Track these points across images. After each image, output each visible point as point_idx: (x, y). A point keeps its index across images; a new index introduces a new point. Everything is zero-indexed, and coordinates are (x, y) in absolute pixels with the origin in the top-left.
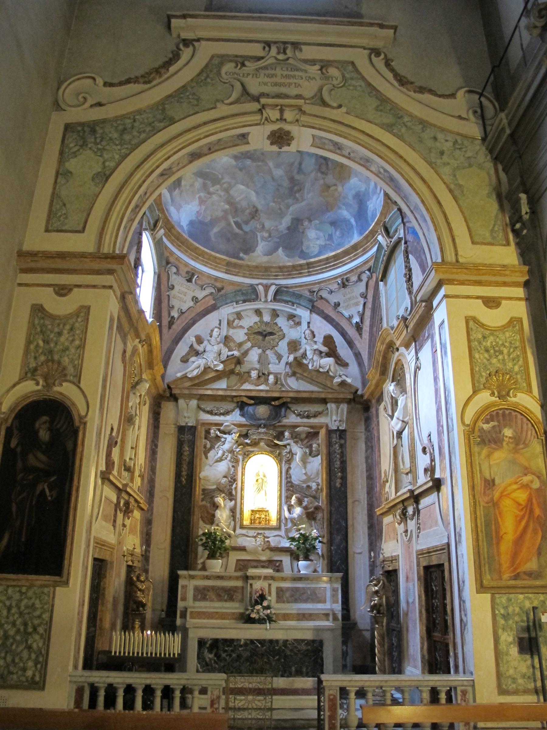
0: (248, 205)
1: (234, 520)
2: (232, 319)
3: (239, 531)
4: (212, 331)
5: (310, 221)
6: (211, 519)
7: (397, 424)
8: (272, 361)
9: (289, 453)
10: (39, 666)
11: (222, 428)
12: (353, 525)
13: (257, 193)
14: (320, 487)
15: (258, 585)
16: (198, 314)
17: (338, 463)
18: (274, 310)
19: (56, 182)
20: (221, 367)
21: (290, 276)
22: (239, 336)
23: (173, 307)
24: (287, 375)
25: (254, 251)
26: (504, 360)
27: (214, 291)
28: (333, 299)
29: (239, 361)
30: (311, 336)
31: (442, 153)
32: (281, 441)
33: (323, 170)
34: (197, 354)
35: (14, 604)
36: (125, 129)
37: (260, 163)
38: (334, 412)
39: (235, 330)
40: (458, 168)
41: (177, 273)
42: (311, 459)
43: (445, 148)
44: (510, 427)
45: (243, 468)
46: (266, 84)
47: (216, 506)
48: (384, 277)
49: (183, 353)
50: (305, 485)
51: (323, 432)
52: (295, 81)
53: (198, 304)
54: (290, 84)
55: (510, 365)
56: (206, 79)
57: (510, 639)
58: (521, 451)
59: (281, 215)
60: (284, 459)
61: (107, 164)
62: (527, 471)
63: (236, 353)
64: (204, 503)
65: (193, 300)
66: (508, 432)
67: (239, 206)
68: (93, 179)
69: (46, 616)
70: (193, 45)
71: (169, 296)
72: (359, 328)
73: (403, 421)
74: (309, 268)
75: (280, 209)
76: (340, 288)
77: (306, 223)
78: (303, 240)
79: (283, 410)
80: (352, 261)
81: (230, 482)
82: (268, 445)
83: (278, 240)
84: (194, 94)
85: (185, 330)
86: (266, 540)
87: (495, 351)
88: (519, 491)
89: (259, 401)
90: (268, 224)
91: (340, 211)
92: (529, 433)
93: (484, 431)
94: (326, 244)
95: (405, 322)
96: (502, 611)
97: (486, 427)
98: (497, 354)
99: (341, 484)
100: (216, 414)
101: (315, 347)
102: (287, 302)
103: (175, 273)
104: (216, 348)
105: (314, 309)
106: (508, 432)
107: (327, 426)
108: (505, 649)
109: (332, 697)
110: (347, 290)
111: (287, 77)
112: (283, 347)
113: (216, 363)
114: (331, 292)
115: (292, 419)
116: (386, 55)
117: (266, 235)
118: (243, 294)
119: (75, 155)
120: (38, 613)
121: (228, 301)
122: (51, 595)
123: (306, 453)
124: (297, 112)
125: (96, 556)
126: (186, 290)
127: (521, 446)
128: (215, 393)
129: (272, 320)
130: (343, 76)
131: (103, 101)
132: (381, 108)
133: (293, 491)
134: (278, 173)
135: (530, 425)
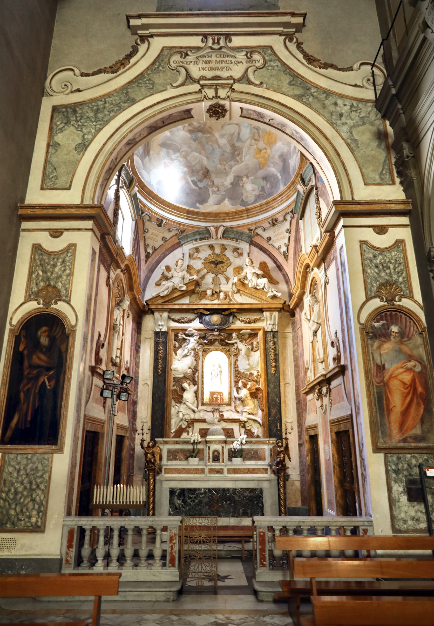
0: (201, 167)
1: (197, 400)
2: (192, 253)
3: (200, 407)
4: (177, 262)
5: (248, 177)
6: (180, 400)
7: (313, 325)
8: (222, 282)
9: (236, 349)
10: (41, 514)
11: (187, 332)
12: (285, 402)
13: (208, 158)
14: (259, 374)
15: (214, 447)
16: (167, 250)
17: (273, 356)
18: (223, 245)
19: (47, 152)
20: (184, 288)
21: (234, 219)
22: (198, 264)
23: (148, 245)
24: (234, 292)
25: (206, 202)
26: (390, 273)
27: (178, 232)
28: (266, 235)
29: (197, 284)
30: (250, 262)
31: (341, 115)
32: (230, 340)
34: (167, 279)
35: (22, 468)
36: (98, 109)
37: (209, 135)
38: (269, 318)
39: (195, 261)
40: (354, 126)
41: (150, 220)
42: (252, 353)
43: (343, 111)
44: (396, 324)
45: (203, 362)
46: (204, 69)
47: (184, 390)
48: (302, 216)
49: (157, 279)
50: (248, 373)
51: (261, 333)
52: (226, 65)
53: (167, 242)
54: (222, 69)
55: (395, 277)
56: (158, 68)
57: (401, 489)
58: (406, 343)
59: (226, 174)
60: (233, 354)
61: (86, 136)
62: (410, 358)
63: (195, 277)
64: (175, 387)
65: (163, 240)
66: (394, 329)
67: (195, 169)
68: (76, 149)
69: (46, 476)
70: (148, 41)
71: (144, 237)
72: (285, 255)
73: (317, 323)
74: (247, 213)
75: (225, 169)
76: (271, 227)
77: (245, 179)
79: (231, 318)
80: (279, 206)
81: (193, 371)
82: (221, 345)
84: (150, 80)
85: (158, 262)
86: (221, 413)
87: (383, 267)
88: (404, 374)
89: (213, 311)
91: (269, 168)
92: (412, 328)
93: (376, 328)
94: (260, 194)
95: (316, 249)
96: (394, 467)
97: (376, 325)
98: (385, 269)
99: (275, 371)
100: (182, 322)
101: (254, 271)
102: (232, 239)
103: (148, 220)
104: (181, 274)
105: (252, 243)
106: (394, 329)
107: (264, 329)
108: (397, 497)
109: (262, 534)
110: (276, 227)
111: (221, 62)
112: (230, 271)
113: (180, 285)
114: (265, 230)
115: (238, 324)
116: (297, 40)
117: (216, 189)
118: (200, 234)
119: (61, 130)
120: (40, 474)
121: (189, 240)
122: (50, 460)
123: (249, 349)
124: (228, 89)
125: (88, 429)
127: (406, 339)
128: (181, 307)
129: (221, 252)
130: (264, 59)
131: (81, 89)
132: (293, 83)
133: (240, 377)
134: (223, 141)
135: (412, 323)
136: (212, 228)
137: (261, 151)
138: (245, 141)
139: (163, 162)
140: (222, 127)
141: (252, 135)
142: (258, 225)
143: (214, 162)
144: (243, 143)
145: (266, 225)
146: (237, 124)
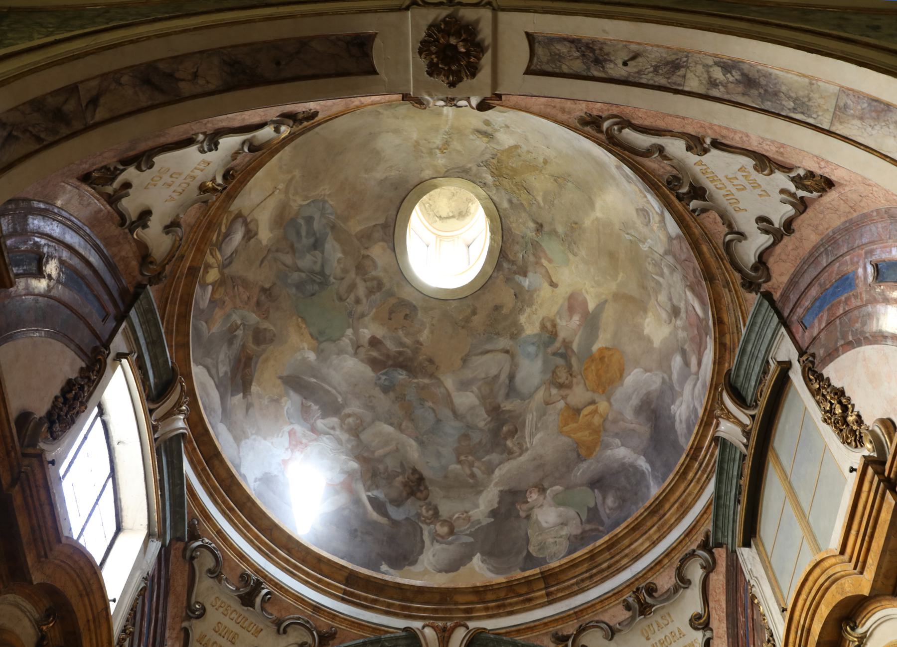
0: (402, 465)
5: (542, 490)
13: (421, 443)
33: (561, 381)
37: (426, 381)
41: (215, 573)
48: (750, 534)
59: (477, 487)
67: (381, 467)
75: (473, 476)
76: (633, 618)
77: (533, 497)
78: (529, 532)
83: (471, 540)
90: (446, 508)
91: (609, 452)
110: (654, 619)
117: (444, 530)
126: (237, 629)
134: (466, 400)
136: (428, 631)
137: (577, 411)
138: (531, 395)
139: (287, 428)
140: (465, 360)
141: (549, 376)
142: (587, 618)
143: (439, 455)
144: (523, 399)
145: (617, 614)
146: (507, 352)
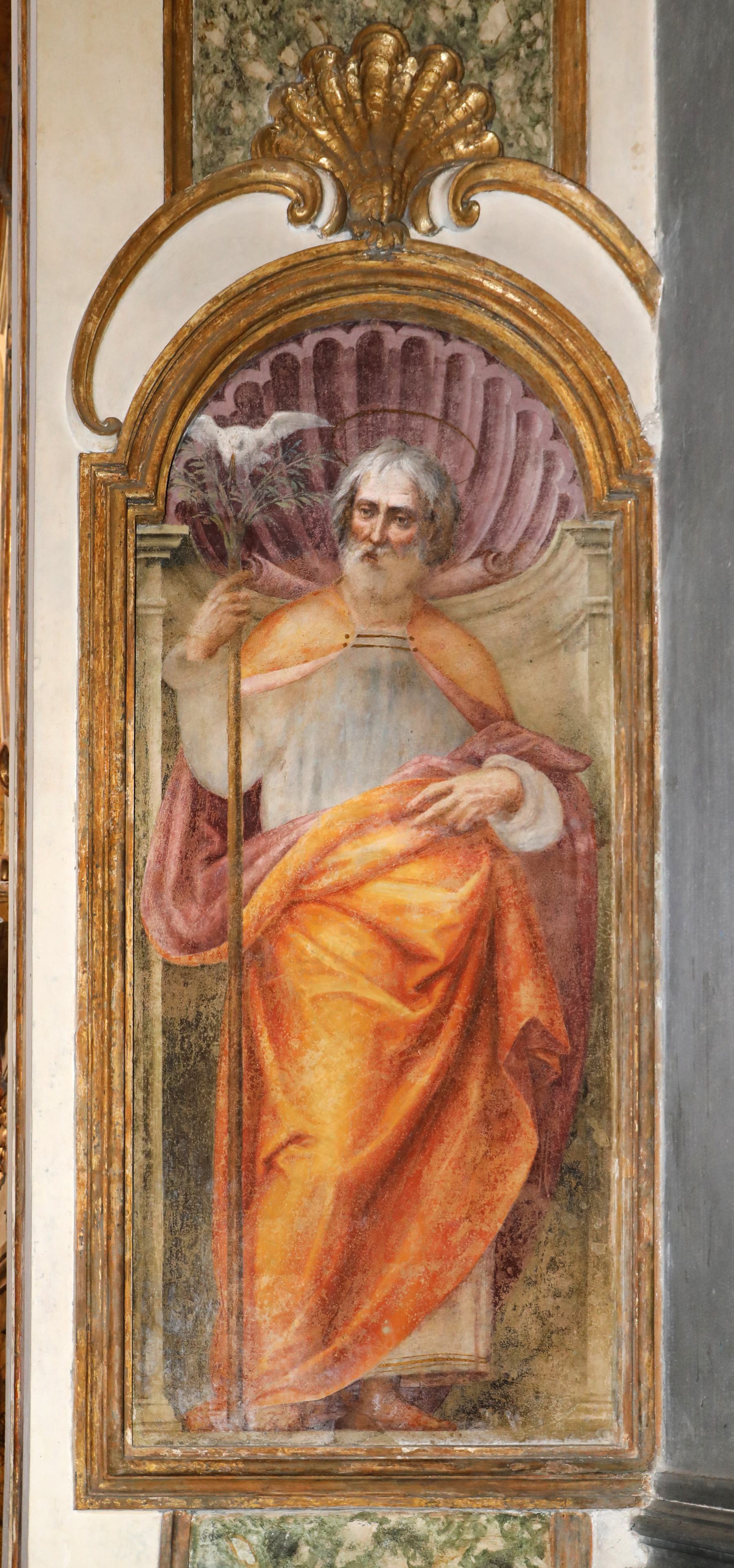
58: (461, 606)
88: (415, 870)
92: (533, 478)
127: (473, 570)
